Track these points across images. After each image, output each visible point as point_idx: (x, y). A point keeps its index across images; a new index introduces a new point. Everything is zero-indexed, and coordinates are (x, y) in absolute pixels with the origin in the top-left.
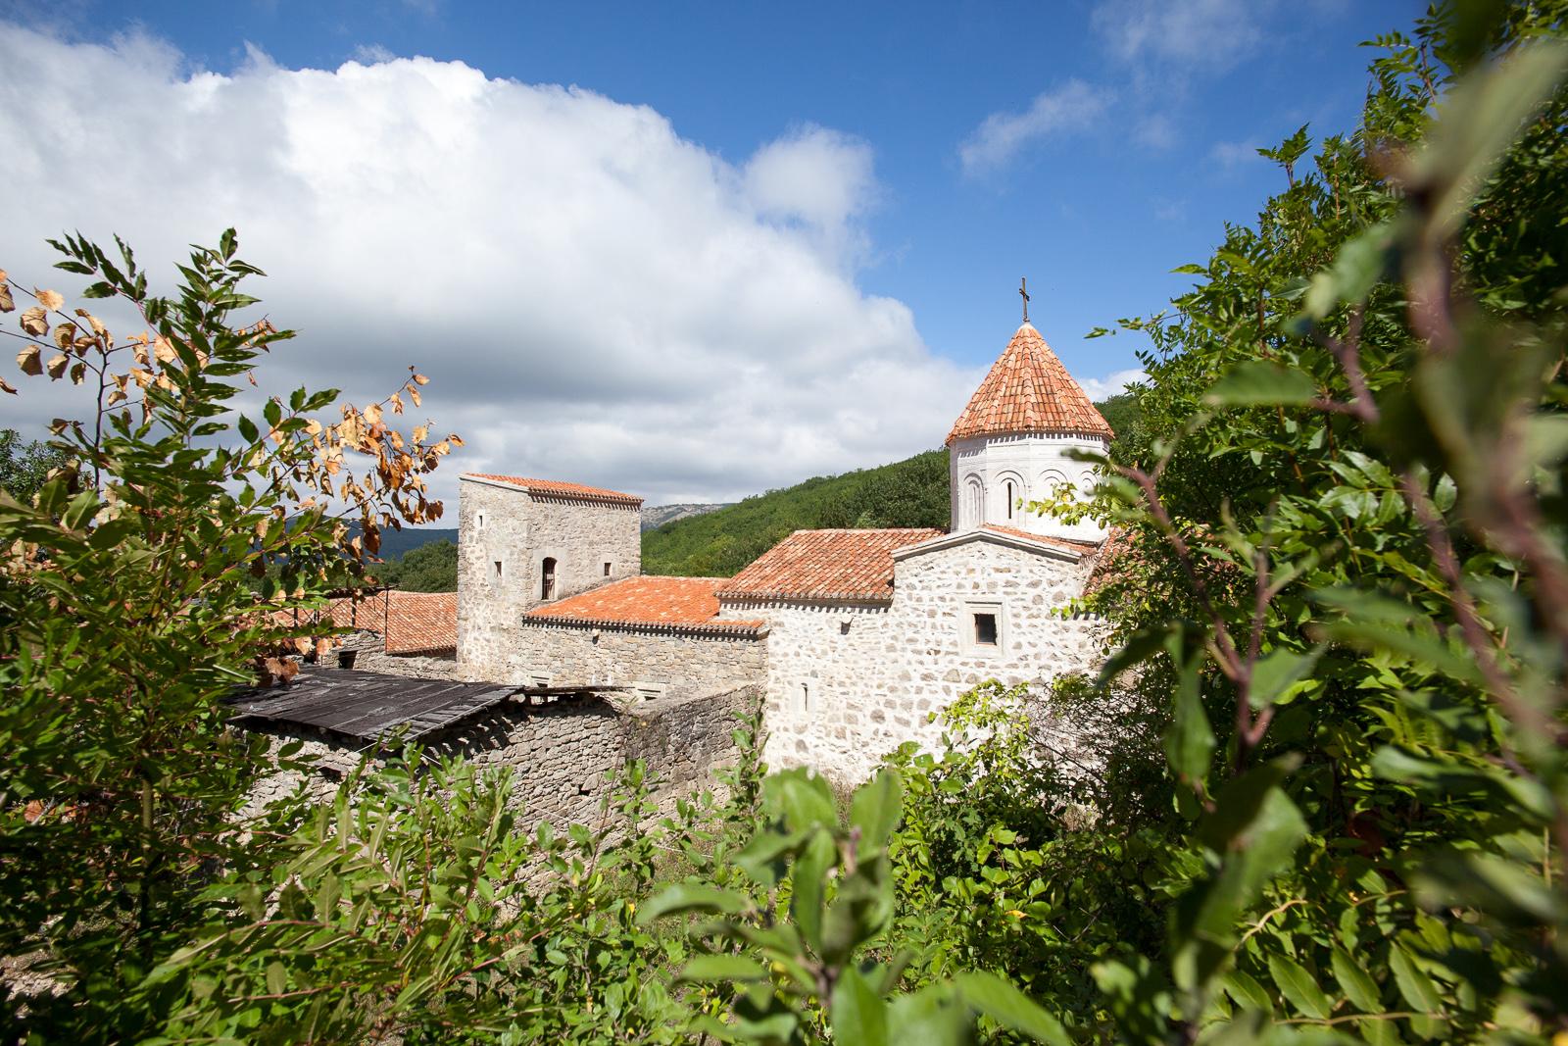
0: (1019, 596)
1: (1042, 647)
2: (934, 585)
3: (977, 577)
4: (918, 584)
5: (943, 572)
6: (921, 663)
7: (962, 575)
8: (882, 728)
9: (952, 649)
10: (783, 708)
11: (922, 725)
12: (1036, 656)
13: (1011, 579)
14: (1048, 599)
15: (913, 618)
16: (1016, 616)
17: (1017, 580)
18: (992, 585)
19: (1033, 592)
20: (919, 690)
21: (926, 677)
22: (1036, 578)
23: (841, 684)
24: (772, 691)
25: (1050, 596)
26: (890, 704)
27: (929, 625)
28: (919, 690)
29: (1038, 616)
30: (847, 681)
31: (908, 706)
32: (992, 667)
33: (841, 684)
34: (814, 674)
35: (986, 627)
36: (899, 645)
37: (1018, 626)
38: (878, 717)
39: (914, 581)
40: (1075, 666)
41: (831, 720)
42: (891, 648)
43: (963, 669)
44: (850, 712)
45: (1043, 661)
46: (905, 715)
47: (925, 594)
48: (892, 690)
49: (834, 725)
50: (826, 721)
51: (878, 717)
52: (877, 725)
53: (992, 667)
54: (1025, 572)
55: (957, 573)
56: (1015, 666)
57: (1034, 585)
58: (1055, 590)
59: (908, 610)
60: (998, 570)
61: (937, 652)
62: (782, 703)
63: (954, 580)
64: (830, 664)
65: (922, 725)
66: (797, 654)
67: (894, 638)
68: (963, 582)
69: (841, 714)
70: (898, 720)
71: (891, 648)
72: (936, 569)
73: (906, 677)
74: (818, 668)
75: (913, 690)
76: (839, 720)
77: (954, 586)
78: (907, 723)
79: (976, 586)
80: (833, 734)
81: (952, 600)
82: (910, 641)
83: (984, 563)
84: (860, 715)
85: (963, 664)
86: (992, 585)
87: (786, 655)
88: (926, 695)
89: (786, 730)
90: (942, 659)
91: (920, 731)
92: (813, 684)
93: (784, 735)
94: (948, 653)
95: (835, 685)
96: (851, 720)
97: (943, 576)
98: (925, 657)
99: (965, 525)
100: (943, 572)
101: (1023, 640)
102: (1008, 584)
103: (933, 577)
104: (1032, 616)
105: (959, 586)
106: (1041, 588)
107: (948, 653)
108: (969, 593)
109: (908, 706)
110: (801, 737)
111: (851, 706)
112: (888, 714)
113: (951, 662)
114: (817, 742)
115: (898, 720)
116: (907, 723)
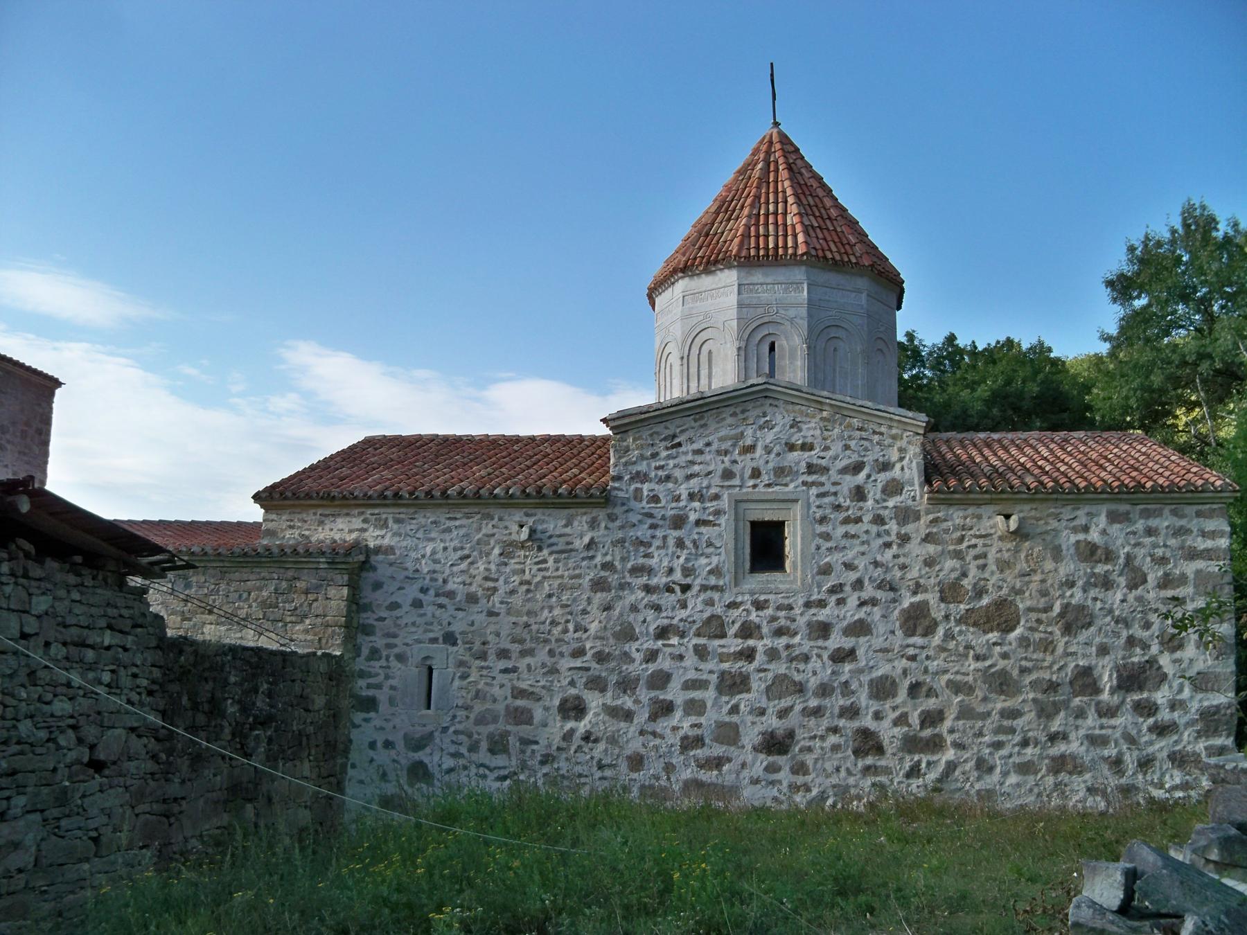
2: (678, 474)
5: (699, 452)
6: (657, 608)
8: (582, 726)
9: (713, 581)
10: (383, 707)
11: (653, 717)
12: (858, 585)
14: (874, 492)
15: (643, 532)
16: (823, 520)
17: (823, 462)
18: (780, 471)
19: (850, 481)
20: (652, 656)
21: (663, 633)
22: (855, 458)
23: (503, 654)
24: (362, 674)
25: (880, 486)
26: (597, 684)
27: (671, 542)
28: (652, 656)
29: (858, 520)
30: (516, 648)
31: (627, 685)
32: (779, 608)
33: (503, 654)
34: (450, 639)
35: (766, 546)
36: (613, 579)
37: (827, 537)
39: (642, 467)
40: (919, 598)
41: (481, 721)
42: (599, 585)
43: (735, 613)
44: (520, 703)
45: (869, 592)
46: (627, 702)
47: (660, 489)
48: (601, 657)
49: (486, 730)
50: (469, 725)
52: (570, 725)
53: (779, 608)
54: (836, 448)
56: (822, 604)
58: (883, 477)
59: (634, 518)
60: (791, 447)
61: (686, 588)
62: (382, 696)
63: (718, 465)
64: (480, 618)
65: (653, 717)
66: (417, 604)
67: (607, 566)
68: (736, 469)
69: (500, 707)
71: (599, 585)
73: (628, 634)
74: (457, 628)
75: (638, 657)
76: (495, 720)
77: (719, 472)
78: (628, 716)
79: (756, 473)
80: (484, 745)
81: (716, 497)
82: (636, 571)
83: (770, 436)
84: (538, 714)
85: (733, 605)
87: (395, 606)
88: (663, 663)
89: (388, 744)
90: (695, 602)
91: (650, 727)
92: (445, 660)
93: (382, 756)
94: (704, 588)
95: (492, 657)
97: (699, 458)
98: (668, 600)
101: (836, 559)
102: (811, 469)
103: (682, 460)
104: (847, 521)
105: (728, 474)
106: (863, 475)
107: (704, 588)
109: (627, 685)
110: (421, 756)
111: (519, 693)
112: (594, 701)
113: (710, 603)
114: (449, 763)
116: (628, 716)
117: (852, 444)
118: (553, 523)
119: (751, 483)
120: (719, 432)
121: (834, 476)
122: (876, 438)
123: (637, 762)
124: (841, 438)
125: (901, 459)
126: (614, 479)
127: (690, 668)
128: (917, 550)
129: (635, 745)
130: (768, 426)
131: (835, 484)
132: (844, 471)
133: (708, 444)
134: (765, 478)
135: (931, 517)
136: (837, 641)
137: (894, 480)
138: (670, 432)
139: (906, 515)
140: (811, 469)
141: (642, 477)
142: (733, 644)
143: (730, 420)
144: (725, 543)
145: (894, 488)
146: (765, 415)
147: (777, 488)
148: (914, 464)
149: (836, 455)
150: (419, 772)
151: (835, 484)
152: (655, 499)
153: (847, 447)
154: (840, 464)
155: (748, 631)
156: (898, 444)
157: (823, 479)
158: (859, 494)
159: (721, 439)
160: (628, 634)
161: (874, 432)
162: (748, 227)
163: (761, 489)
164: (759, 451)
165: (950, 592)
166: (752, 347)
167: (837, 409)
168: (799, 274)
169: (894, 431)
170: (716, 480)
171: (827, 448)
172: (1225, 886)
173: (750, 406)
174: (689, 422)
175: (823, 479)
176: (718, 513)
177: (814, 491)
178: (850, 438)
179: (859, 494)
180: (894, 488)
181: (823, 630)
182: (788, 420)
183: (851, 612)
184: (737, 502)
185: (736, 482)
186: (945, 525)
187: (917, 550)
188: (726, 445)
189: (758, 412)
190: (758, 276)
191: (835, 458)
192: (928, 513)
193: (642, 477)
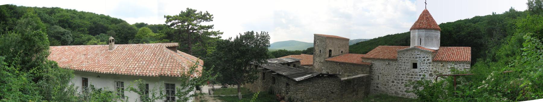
1: (425, 69)
3: (414, 56)
18: (417, 58)
26: (396, 80)
31: (399, 80)
35: (415, 66)
38: (393, 82)
42: (396, 69)
51: (393, 82)
63: (409, 56)
70: (397, 83)
71: (396, 69)
73: (399, 75)
86: (417, 58)
92: (380, 75)
96: (388, 82)
99: (411, 46)
108: (412, 59)
109: (399, 80)
112: (395, 81)
115: (397, 83)
118: (391, 62)
120: (409, 53)
123: (400, 88)
127: (405, 79)
128: (431, 67)
129: (399, 86)
136: (422, 77)
139: (430, 63)
142: (410, 76)
144: (410, 65)
145: (428, 60)
149: (422, 56)
150: (377, 87)
155: (412, 75)
158: (424, 60)
160: (399, 75)
165: (435, 72)
168: (424, 30)
179: (424, 60)
180: (428, 60)
181: (420, 75)
183: (423, 73)
187: (431, 67)
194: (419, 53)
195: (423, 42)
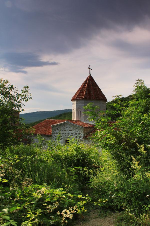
0: (73, 136)
4: (56, 133)
7: (64, 131)
13: (72, 133)
17: (73, 133)
18: (68, 134)
22: (76, 132)
39: (55, 132)
55: (63, 131)
57: (76, 134)
58: (79, 135)
59: (54, 138)
60: (69, 130)
63: (62, 132)
68: (64, 133)
72: (59, 130)
79: (66, 134)
81: (62, 136)
83: (67, 129)
86: (68, 134)
100: (60, 130)
102: (71, 134)
117: (76, 130)
119: (65, 135)
120: (62, 128)
121: (74, 135)
122: (79, 130)
124: (75, 130)
125: (81, 133)
126: (52, 133)
130: (67, 127)
131: (74, 136)
132: (75, 134)
133: (61, 129)
134: (67, 134)
135: (84, 141)
137: (80, 136)
138: (57, 128)
140: (71, 134)
141: (55, 133)
143: (63, 127)
146: (67, 126)
147: (68, 136)
148: (82, 134)
151: (74, 136)
152: (56, 136)
153: (75, 131)
154: (75, 133)
156: (81, 131)
157: (73, 135)
159: (62, 129)
161: (78, 129)
162: (79, 94)
163: (66, 136)
164: (66, 131)
166: (78, 112)
167: (74, 126)
168: (83, 101)
169: (81, 129)
170: (62, 134)
171: (73, 131)
172: (28, 217)
173: (65, 125)
174: (59, 127)
175: (73, 135)
176: (62, 138)
177: (72, 136)
178: (76, 130)
180: (80, 137)
182: (69, 127)
184: (64, 137)
185: (64, 135)
186: (86, 143)
188: (63, 130)
189: (66, 126)
190: (79, 102)
191: (74, 132)
192: (84, 141)
193: (55, 133)
194: (71, 129)
195: (83, 115)
